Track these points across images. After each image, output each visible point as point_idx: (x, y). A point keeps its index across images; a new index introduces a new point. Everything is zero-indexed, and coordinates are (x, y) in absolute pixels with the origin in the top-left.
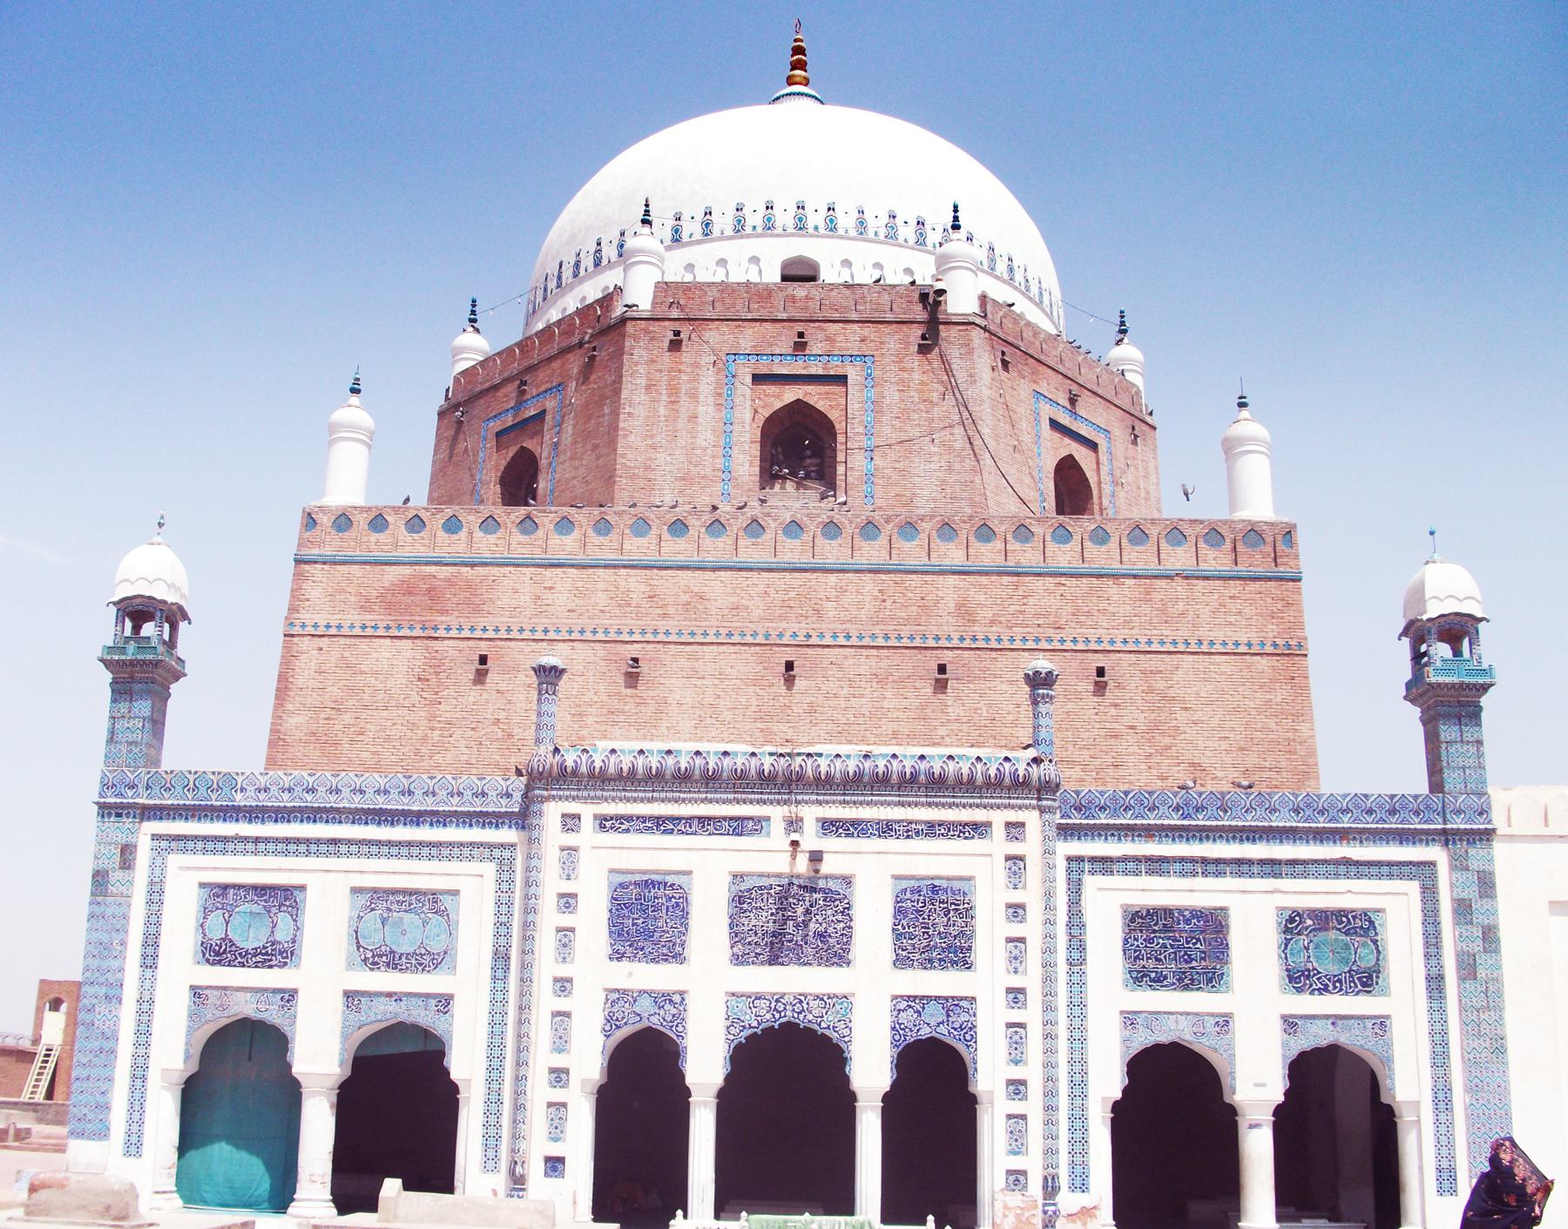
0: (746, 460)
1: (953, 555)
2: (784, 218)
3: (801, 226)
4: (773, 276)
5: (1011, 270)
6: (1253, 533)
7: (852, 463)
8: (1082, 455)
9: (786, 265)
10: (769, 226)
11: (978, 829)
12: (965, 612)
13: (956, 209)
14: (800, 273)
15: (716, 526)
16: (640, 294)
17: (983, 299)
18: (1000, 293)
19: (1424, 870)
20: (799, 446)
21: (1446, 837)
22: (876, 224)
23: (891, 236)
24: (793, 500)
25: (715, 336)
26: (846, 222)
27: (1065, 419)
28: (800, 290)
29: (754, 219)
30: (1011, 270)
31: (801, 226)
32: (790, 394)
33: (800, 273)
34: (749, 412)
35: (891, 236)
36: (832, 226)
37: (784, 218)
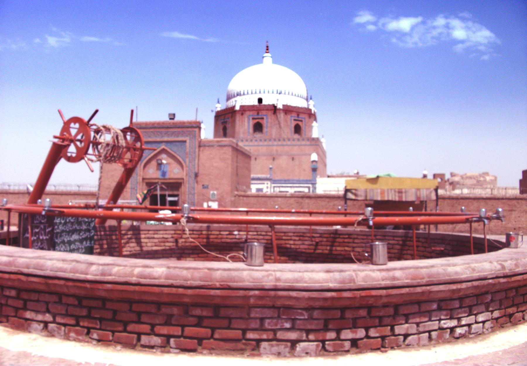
0: (251, 130)
1: (275, 143)
2: (258, 92)
6: (313, 139)
7: (265, 130)
8: (300, 123)
10: (256, 93)
11: (264, 184)
12: (277, 151)
15: (247, 141)
16: (237, 108)
19: (309, 188)
20: (258, 127)
21: (312, 184)
24: (258, 135)
25: (247, 113)
29: (254, 92)
32: (257, 121)
34: (252, 123)
37: (258, 92)
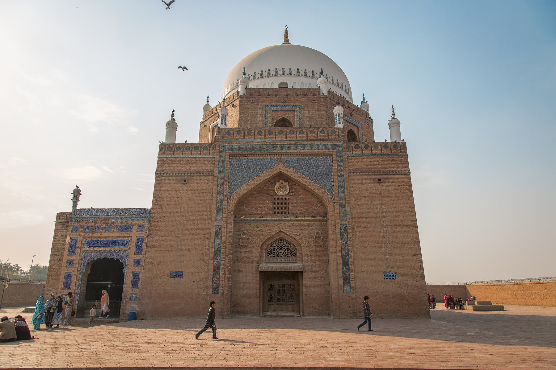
3: (283, 73)
4: (277, 86)
5: (338, 83)
9: (280, 84)
13: (322, 70)
14: (283, 86)
17: (329, 91)
18: (334, 89)
22: (302, 73)
23: (306, 75)
26: (294, 72)
27: (349, 120)
28: (284, 90)
30: (338, 83)
31: (283, 73)
33: (283, 86)
35: (306, 75)
36: (290, 73)
